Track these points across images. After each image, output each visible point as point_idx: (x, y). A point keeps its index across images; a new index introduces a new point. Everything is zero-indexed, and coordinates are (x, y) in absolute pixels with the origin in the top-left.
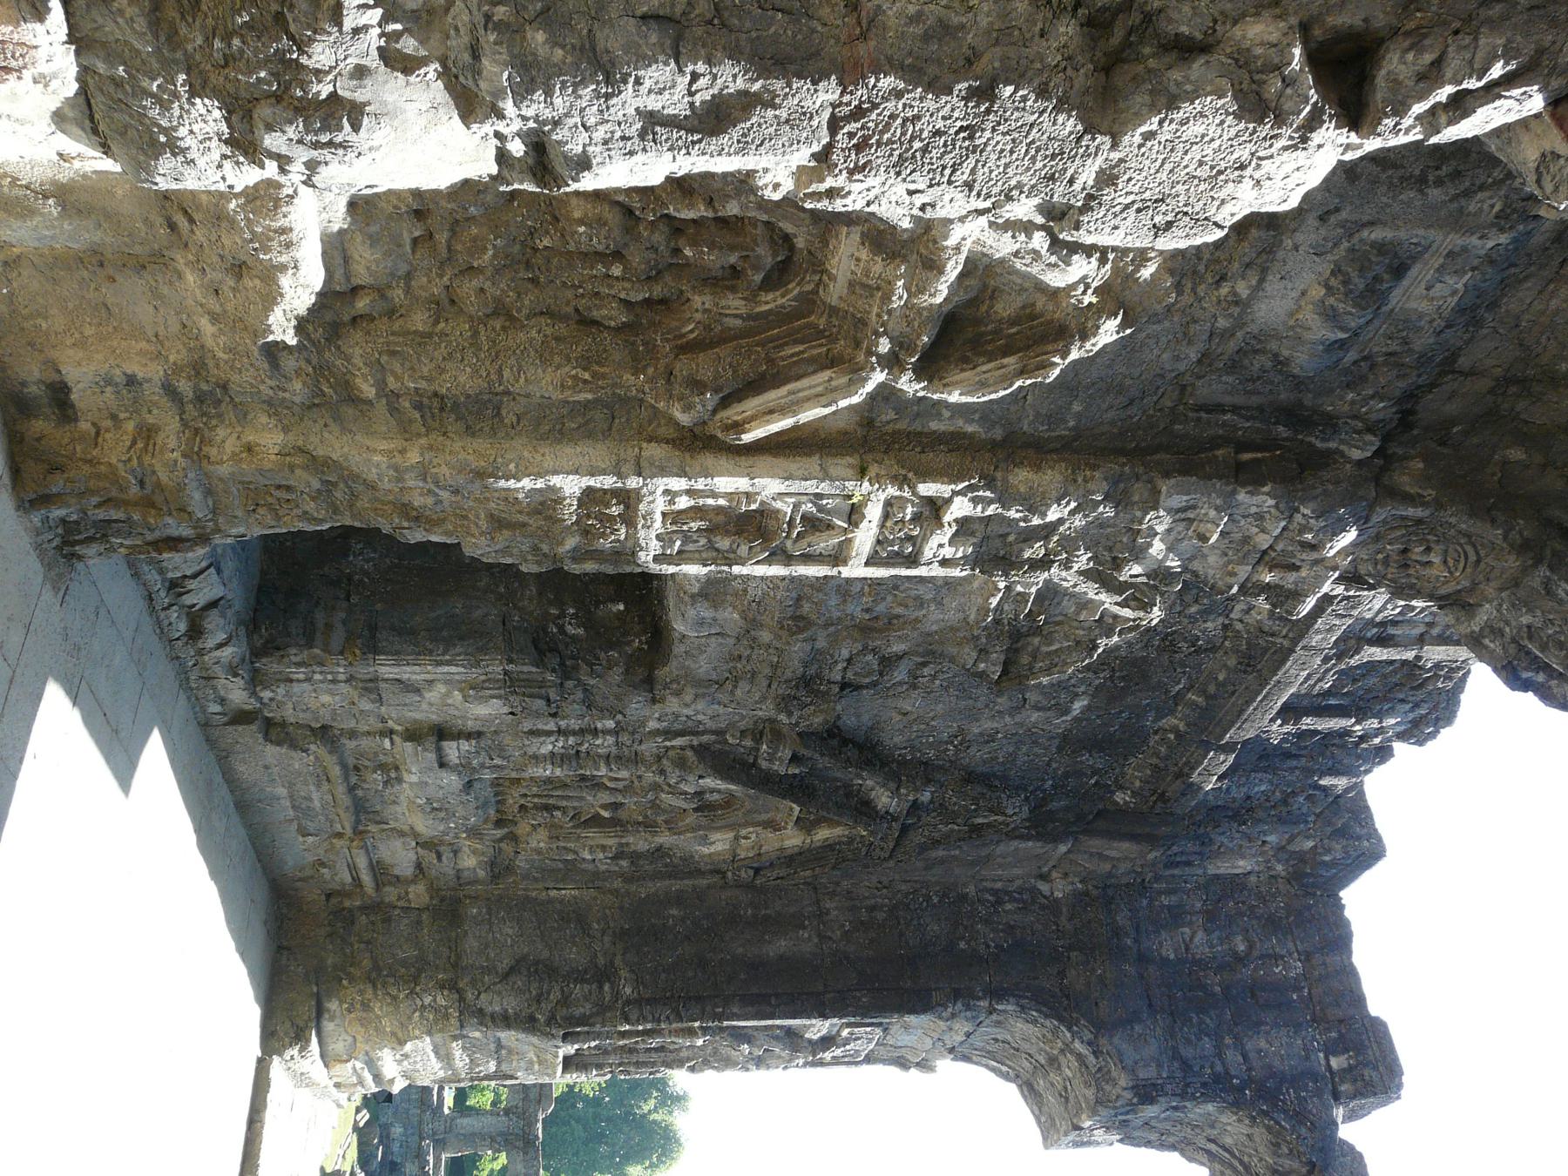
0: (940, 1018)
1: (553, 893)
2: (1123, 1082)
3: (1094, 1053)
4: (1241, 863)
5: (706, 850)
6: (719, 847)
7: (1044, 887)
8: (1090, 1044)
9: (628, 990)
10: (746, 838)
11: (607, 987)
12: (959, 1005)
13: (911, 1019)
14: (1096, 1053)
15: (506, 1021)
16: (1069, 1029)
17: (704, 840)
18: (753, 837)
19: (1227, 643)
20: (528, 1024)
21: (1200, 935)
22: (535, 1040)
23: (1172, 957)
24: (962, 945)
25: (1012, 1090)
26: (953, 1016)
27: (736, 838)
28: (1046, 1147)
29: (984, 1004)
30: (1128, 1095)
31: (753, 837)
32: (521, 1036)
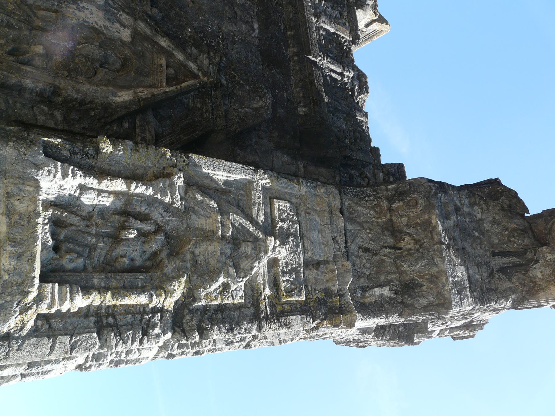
5: (118, 100)
17: (115, 95)
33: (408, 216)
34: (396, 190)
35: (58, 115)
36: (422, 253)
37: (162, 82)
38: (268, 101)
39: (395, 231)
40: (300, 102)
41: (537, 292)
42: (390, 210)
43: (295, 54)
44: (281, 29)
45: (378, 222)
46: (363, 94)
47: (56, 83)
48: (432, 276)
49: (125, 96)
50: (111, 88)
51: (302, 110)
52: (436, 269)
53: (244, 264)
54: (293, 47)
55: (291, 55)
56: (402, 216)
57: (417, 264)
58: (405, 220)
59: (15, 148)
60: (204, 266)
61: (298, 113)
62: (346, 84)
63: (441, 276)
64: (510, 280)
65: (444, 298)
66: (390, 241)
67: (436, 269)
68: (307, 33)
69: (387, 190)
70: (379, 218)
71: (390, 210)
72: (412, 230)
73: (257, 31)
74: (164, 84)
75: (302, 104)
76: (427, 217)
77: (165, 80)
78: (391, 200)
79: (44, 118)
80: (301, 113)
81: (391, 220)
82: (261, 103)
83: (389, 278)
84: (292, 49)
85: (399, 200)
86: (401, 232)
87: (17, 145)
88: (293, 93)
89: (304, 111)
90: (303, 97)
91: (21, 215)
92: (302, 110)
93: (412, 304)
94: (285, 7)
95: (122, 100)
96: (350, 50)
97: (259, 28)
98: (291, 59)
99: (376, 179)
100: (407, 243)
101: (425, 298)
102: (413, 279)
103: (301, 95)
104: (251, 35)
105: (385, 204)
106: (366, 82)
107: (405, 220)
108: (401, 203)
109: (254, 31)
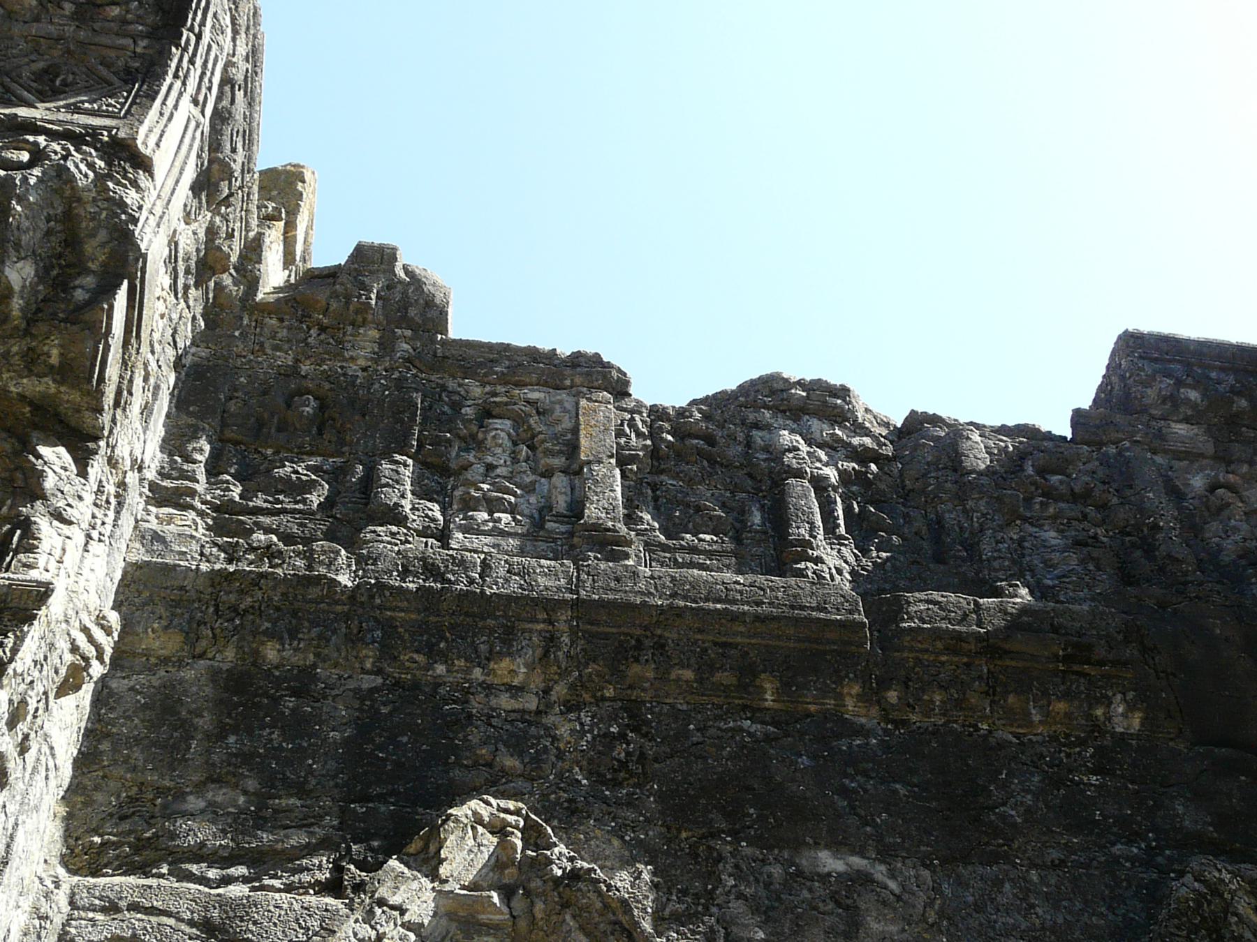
19: (609, 692)
38: (1227, 877)
40: (1089, 716)
43: (872, 696)
44: (768, 738)
46: (853, 411)
51: (1124, 718)
54: (840, 697)
55: (875, 711)
61: (1137, 736)
62: (842, 473)
68: (757, 618)
73: (857, 861)
75: (1099, 712)
80: (1136, 722)
84: (850, 704)
88: (1054, 738)
89: (1131, 707)
90: (1067, 696)
92: (1124, 718)
94: (634, 694)
96: (657, 413)
97: (838, 845)
98: (894, 715)
99: (1202, 456)
103: (1061, 706)
104: (899, 898)
106: (800, 384)
109: (863, 880)
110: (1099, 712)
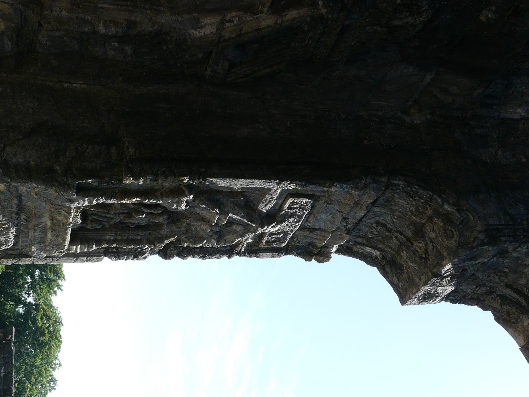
0: (356, 188)
1: (66, 85)
2: (479, 228)
3: (457, 210)
4: (519, 110)
5: (197, 33)
6: (208, 30)
7: (407, 119)
8: (454, 205)
9: (131, 151)
10: (230, 21)
11: (113, 150)
12: (369, 179)
13: (336, 190)
14: (459, 211)
15: (27, 173)
16: (440, 197)
18: (236, 20)
20: (47, 176)
21: (500, 152)
22: (52, 192)
23: (488, 161)
24: (366, 142)
25: (373, 273)
26: (366, 186)
27: (222, 22)
28: (403, 301)
29: (384, 179)
30: (482, 236)
31: (236, 20)
32: (41, 188)
33: (437, 237)
34: (448, 213)
35: (128, 49)
36: (421, 263)
37: (264, 6)
38: (421, 19)
39: (419, 232)
41: (511, 327)
42: (430, 219)
45: (411, 217)
47: (132, 18)
48: (413, 279)
49: (208, 27)
50: (195, 15)
52: (417, 280)
53: (228, 237)
56: (433, 231)
57: (413, 263)
58: (433, 235)
59: (56, 192)
60: (194, 233)
63: (416, 288)
64: (501, 305)
65: (405, 295)
66: (409, 234)
67: (417, 280)
69: (442, 206)
70: (415, 216)
71: (430, 219)
72: (430, 247)
74: (265, 10)
75: (493, 8)
76: (445, 254)
77: (268, 5)
78: (437, 213)
79: (114, 53)
80: (483, 18)
81: (424, 225)
82: (410, 19)
83: (386, 249)
85: (443, 221)
86: (423, 236)
87: (58, 189)
91: (58, 221)
93: (388, 273)
95: (202, 34)
100: (419, 246)
101: (399, 280)
102: (402, 265)
105: (430, 212)
107: (433, 235)
108: (442, 224)
110: (493, 8)
